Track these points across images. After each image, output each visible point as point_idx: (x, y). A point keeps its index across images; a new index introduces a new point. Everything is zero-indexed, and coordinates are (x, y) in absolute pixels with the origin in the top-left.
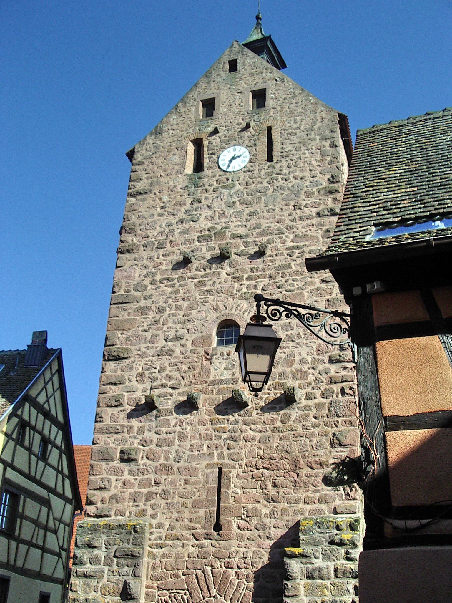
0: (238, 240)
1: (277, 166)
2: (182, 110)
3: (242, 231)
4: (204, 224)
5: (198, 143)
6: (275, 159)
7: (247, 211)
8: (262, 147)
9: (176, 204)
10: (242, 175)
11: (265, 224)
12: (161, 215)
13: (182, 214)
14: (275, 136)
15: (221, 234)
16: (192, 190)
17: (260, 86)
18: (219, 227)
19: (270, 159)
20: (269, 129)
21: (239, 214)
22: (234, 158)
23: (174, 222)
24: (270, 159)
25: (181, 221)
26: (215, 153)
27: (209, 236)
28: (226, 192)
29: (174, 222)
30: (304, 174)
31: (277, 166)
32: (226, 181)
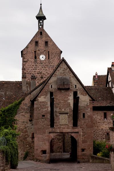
0: (44, 75)
1: (50, 60)
2: (32, 43)
3: (44, 73)
4: (37, 71)
5: (35, 52)
6: (50, 59)
7: (45, 69)
8: (47, 56)
9: (32, 65)
10: (44, 61)
11: (48, 72)
12: (30, 67)
13: (34, 68)
14: (50, 54)
15: (41, 73)
16: (35, 63)
17: (47, 41)
18: (40, 72)
19: (49, 59)
20: (49, 52)
21: (44, 69)
22: (42, 57)
23: (32, 69)
24: (49, 59)
25: (33, 69)
26: (39, 55)
27: (39, 73)
28: (41, 64)
29: (32, 69)
30: (55, 63)
31: (50, 60)
32: (41, 62)
